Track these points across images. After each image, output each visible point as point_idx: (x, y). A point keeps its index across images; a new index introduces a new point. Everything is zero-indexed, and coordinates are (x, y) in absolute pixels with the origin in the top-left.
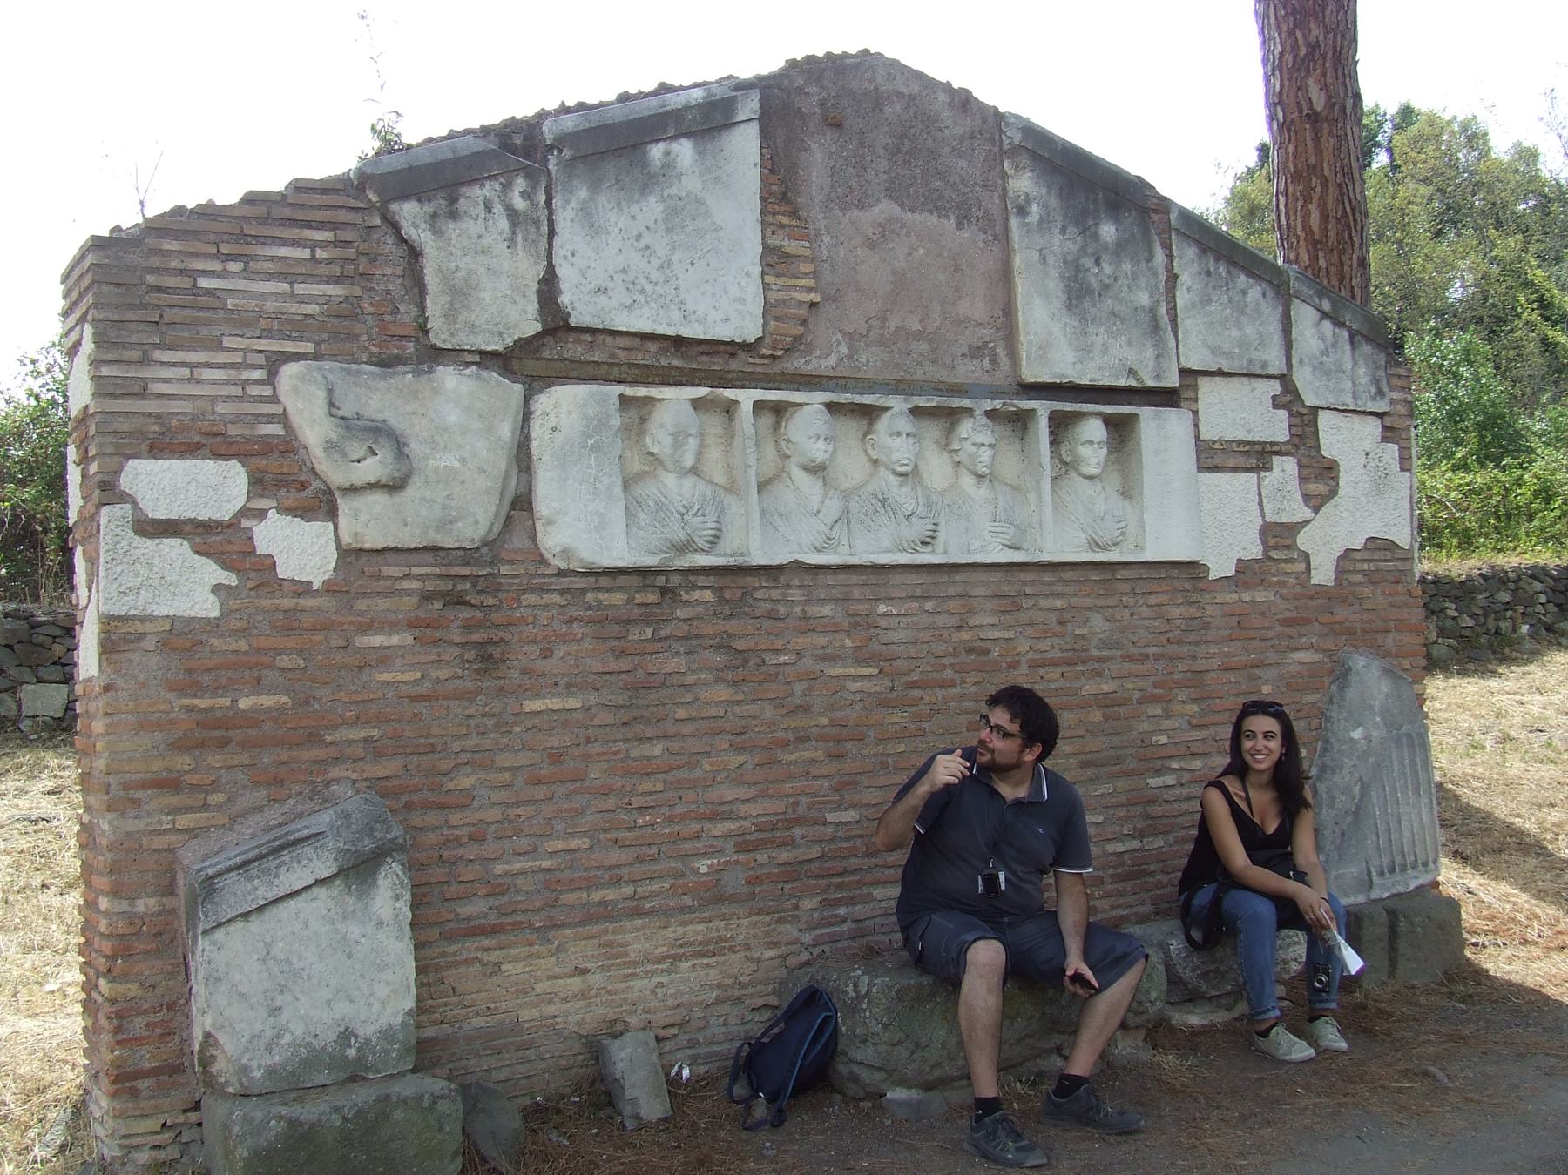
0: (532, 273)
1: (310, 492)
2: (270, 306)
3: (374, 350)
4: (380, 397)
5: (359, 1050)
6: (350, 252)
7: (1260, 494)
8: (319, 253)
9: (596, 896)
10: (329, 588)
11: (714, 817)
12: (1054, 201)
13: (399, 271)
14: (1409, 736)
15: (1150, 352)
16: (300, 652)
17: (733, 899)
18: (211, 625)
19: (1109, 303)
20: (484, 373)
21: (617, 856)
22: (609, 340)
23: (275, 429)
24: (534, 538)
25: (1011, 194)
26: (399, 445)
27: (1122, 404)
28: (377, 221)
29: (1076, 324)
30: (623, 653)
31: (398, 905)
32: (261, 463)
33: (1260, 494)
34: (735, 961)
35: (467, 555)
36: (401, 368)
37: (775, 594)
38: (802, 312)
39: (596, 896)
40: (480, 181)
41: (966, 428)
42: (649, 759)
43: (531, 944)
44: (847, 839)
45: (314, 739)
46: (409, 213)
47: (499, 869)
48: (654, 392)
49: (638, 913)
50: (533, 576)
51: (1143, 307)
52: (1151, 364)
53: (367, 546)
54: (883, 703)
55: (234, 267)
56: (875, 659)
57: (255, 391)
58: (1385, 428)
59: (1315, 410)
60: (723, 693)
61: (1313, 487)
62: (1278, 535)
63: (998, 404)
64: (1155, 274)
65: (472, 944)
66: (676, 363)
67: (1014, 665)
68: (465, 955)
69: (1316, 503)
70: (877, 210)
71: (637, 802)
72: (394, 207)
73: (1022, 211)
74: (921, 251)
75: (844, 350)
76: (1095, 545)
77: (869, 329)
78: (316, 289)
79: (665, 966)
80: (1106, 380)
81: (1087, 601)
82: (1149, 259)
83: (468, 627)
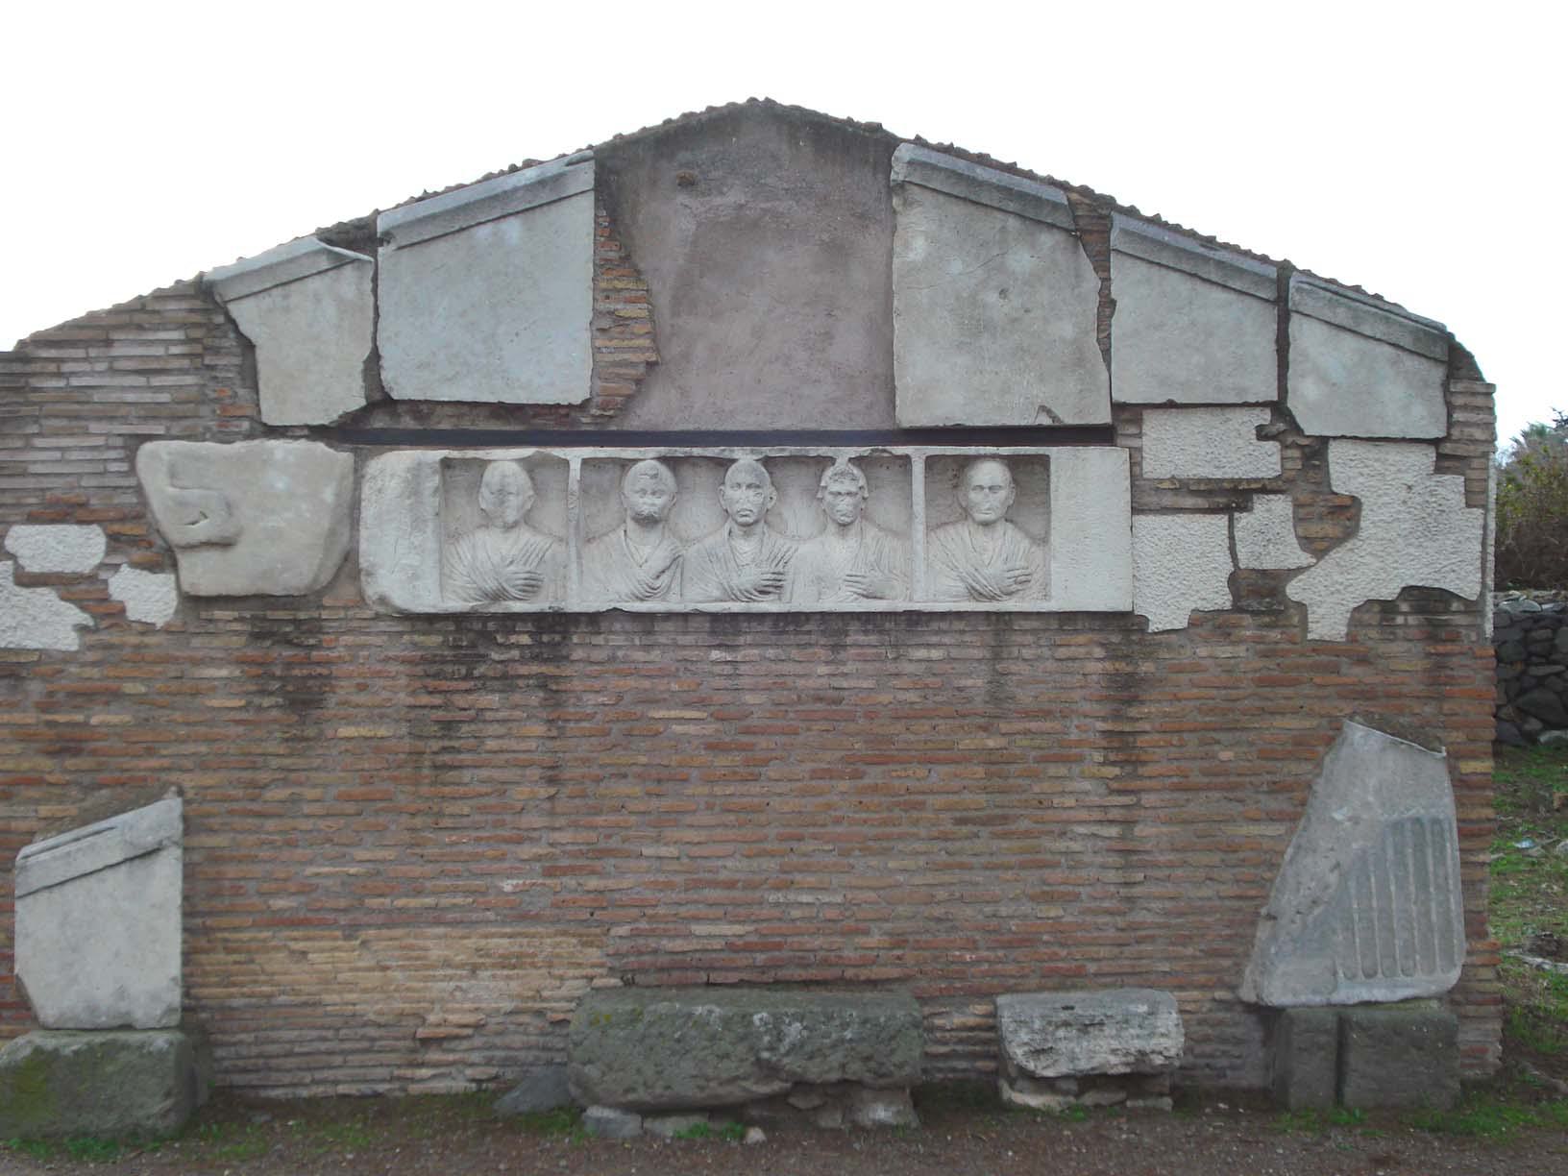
7: (1232, 537)
10: (167, 630)
14: (1417, 820)
16: (143, 680)
17: (536, 918)
18: (68, 658)
27: (1030, 445)
32: (116, 527)
33: (1232, 537)
34: (536, 978)
43: (335, 939)
53: (202, 593)
55: (102, 366)
56: (702, 703)
57: (114, 467)
59: (1324, 441)
61: (1315, 529)
69: (1318, 547)
76: (975, 594)
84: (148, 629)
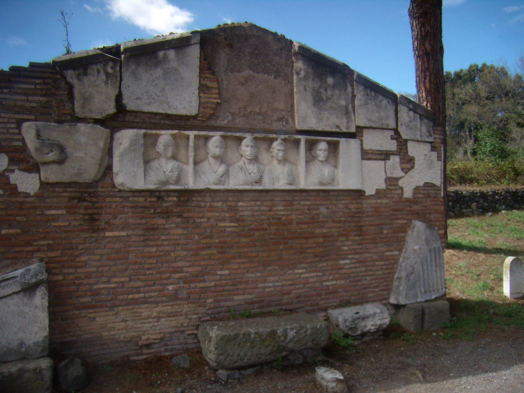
0: (113, 93)
1: (30, 164)
2: (19, 103)
3: (56, 118)
4: (56, 133)
5: (26, 349)
6: (49, 86)
8: (38, 87)
9: (130, 297)
10: (36, 195)
11: (175, 272)
12: (310, 70)
13: (66, 93)
14: (435, 248)
15: (345, 120)
16: (25, 216)
17: (182, 299)
19: (330, 104)
20: (95, 126)
21: (139, 284)
22: (142, 115)
23: (19, 144)
24: (112, 179)
25: (295, 68)
26: (62, 149)
28: (59, 76)
29: (317, 110)
30: (142, 218)
31: (43, 301)
34: (182, 319)
35: (88, 185)
36: (65, 124)
37: (200, 199)
38: (213, 106)
39: (130, 297)
40: (96, 64)
41: (275, 145)
42: (151, 252)
43: (107, 312)
44: (225, 280)
45: (29, 244)
46: (70, 75)
47: (95, 287)
48: (158, 132)
49: (145, 302)
50: (111, 191)
51: (342, 106)
52: (345, 124)
53: (51, 181)
54: (240, 236)
56: (238, 221)
57: (12, 131)
58: (432, 147)
59: (406, 141)
60: (180, 231)
61: (405, 166)
62: (392, 182)
63: (287, 136)
64: (347, 95)
65: (85, 311)
66: (167, 122)
67: (290, 223)
68: (83, 315)
70: (244, 73)
71: (146, 266)
72: (64, 72)
73: (298, 73)
74: (261, 86)
75: (230, 118)
77: (240, 112)
78: (36, 98)
79: (155, 320)
80: (328, 129)
81: (319, 202)
82: (346, 89)
83: (86, 208)
84: (27, 195)
